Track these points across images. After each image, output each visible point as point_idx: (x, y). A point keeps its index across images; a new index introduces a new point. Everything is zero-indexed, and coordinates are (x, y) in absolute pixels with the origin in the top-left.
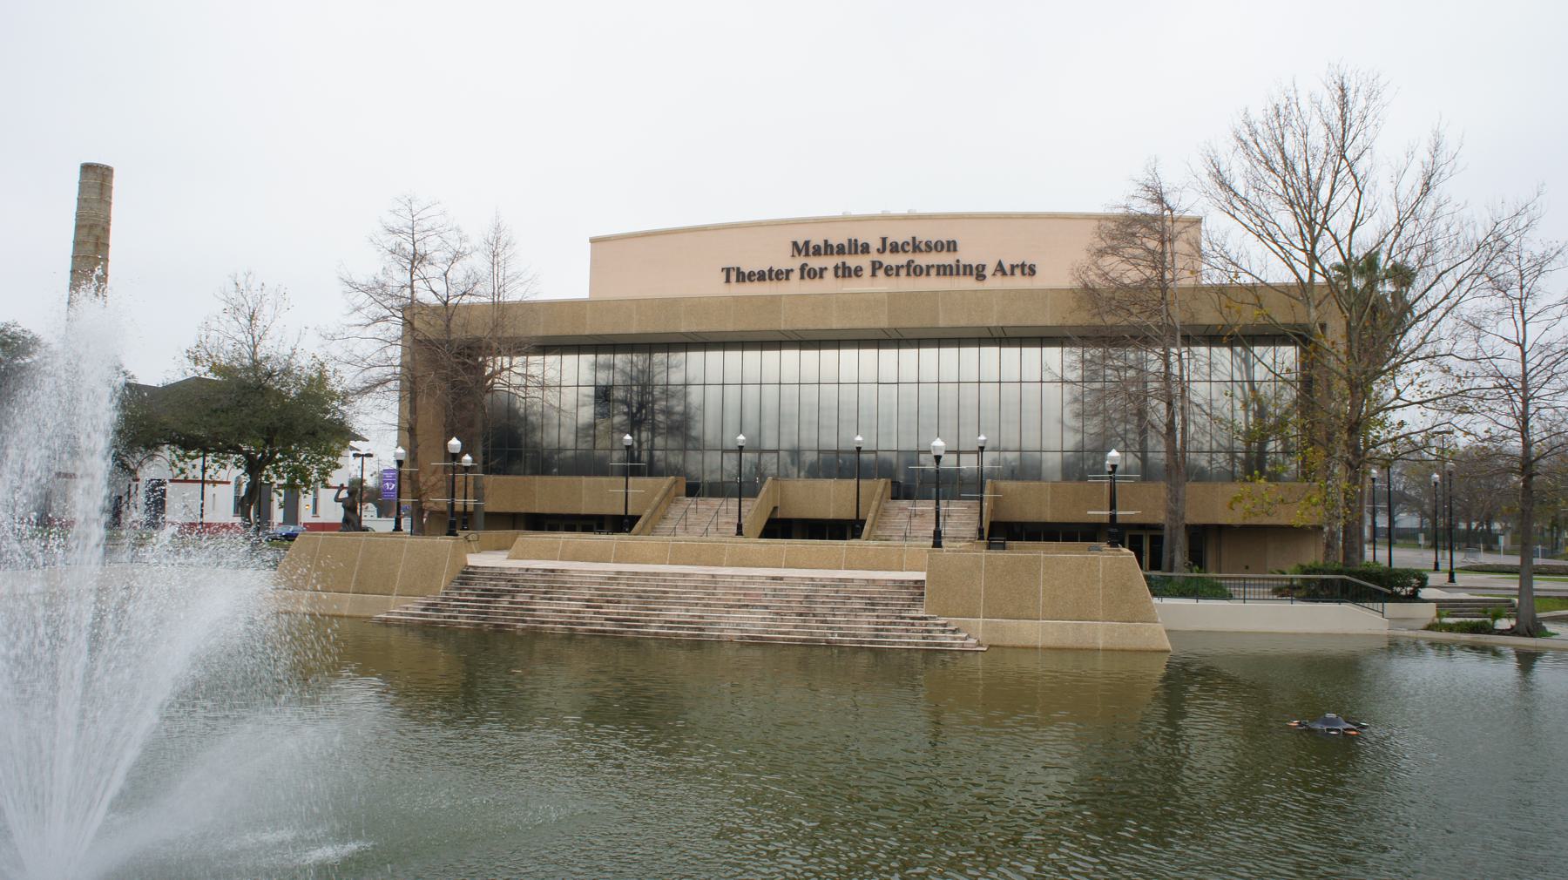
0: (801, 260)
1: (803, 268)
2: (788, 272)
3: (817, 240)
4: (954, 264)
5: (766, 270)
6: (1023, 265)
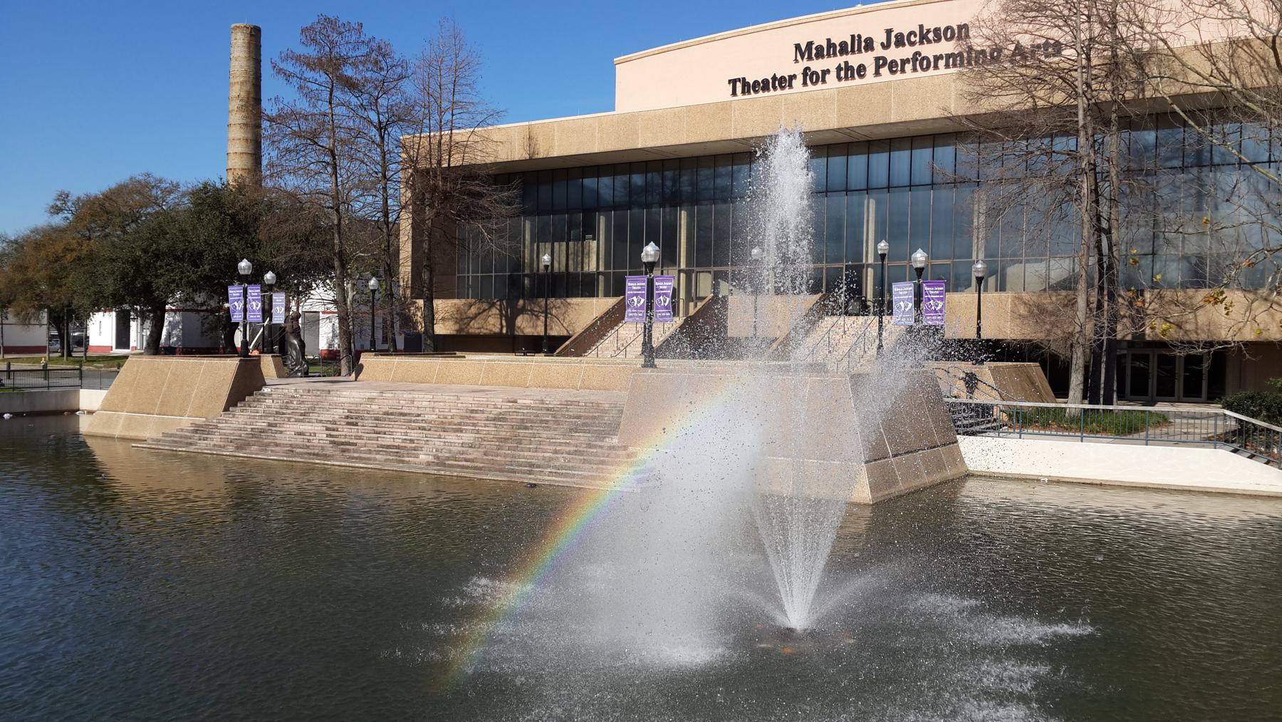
0: (805, 63)
2: (793, 77)
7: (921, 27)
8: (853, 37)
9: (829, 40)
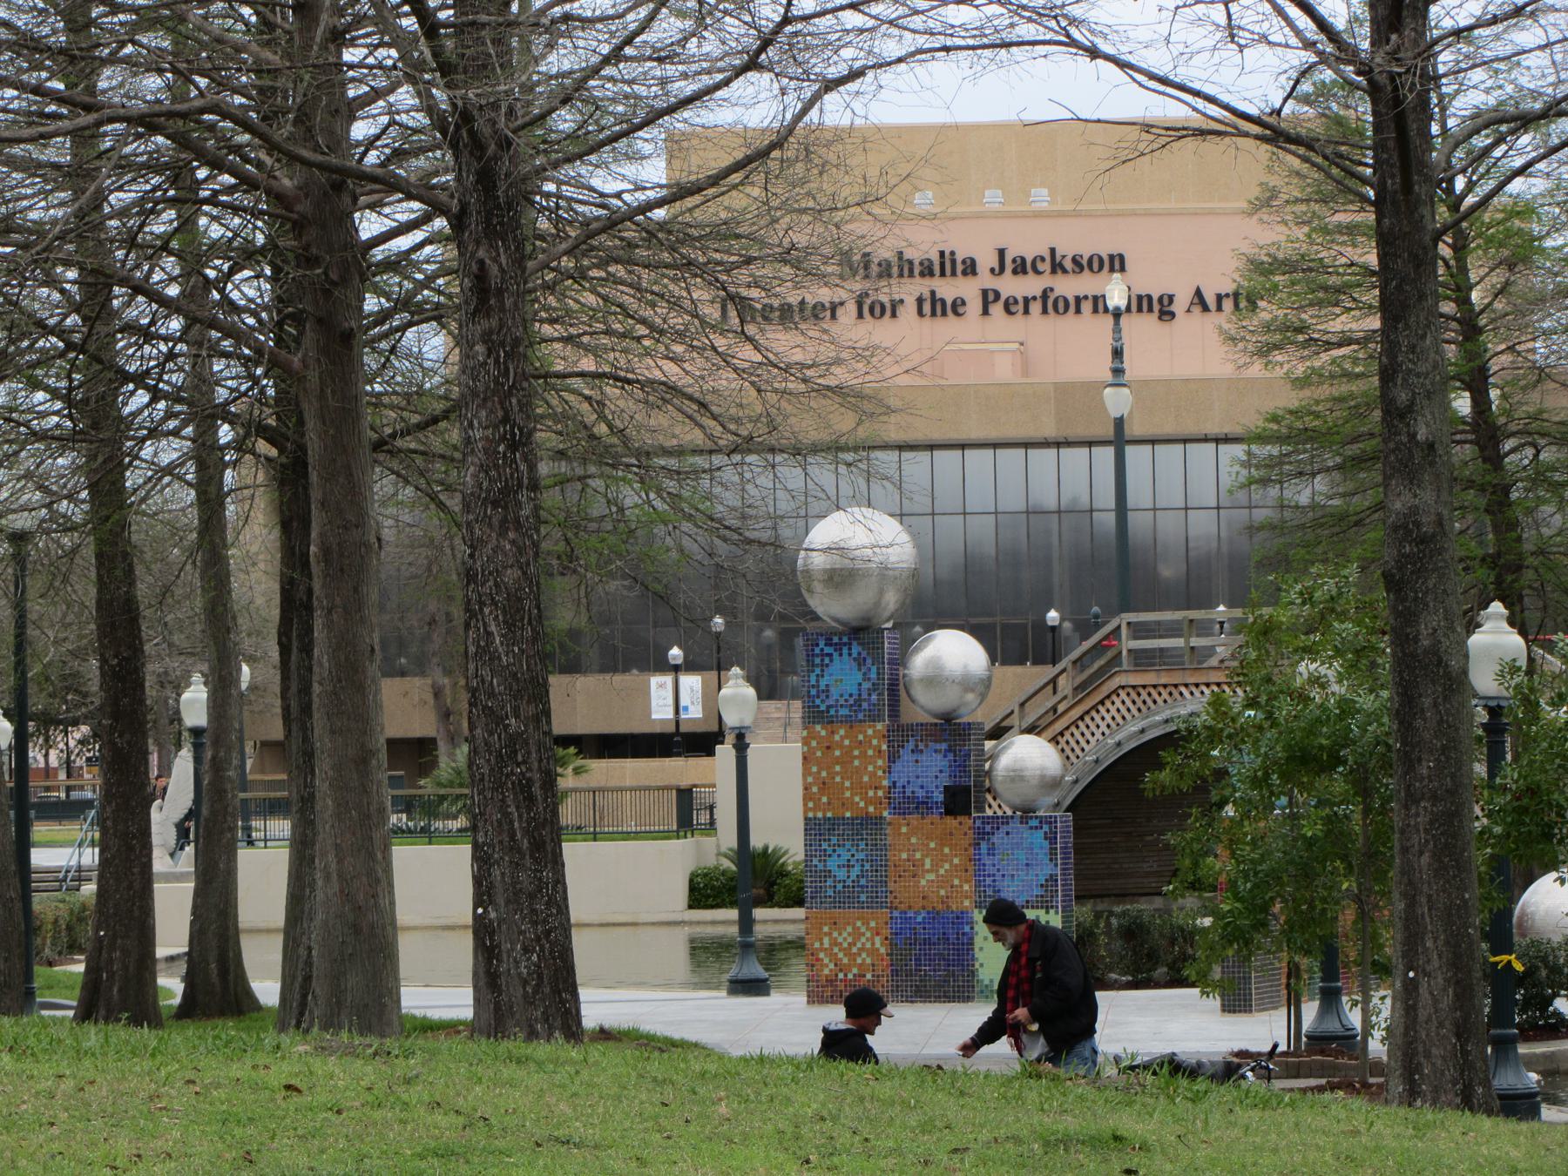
7: (1053, 251)
8: (942, 254)
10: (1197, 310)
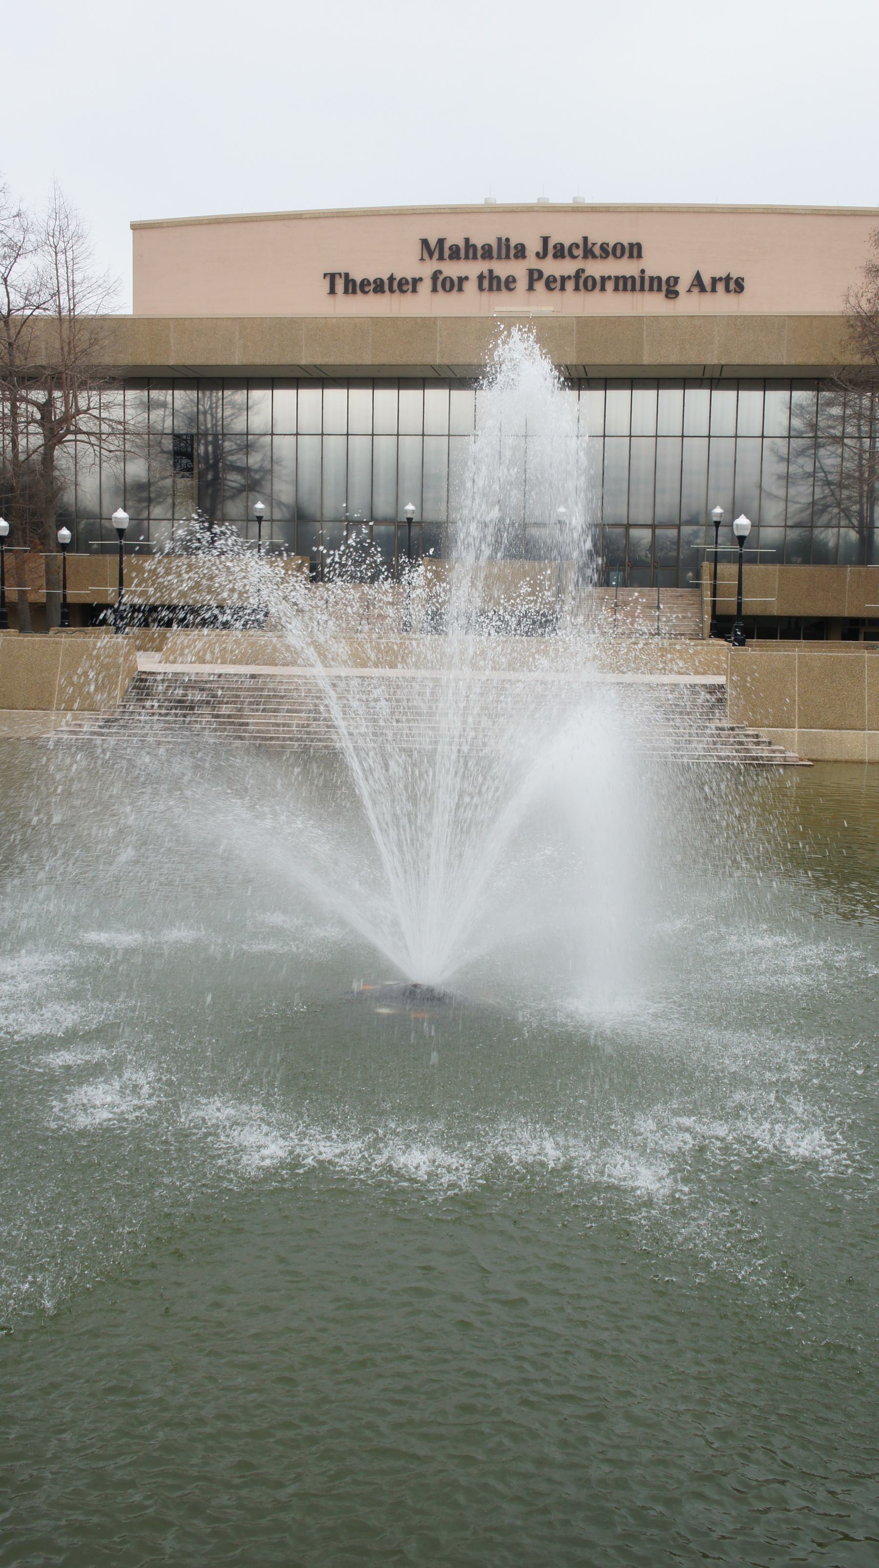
0: (433, 265)
1: (435, 276)
2: (416, 281)
3: (455, 238)
4: (637, 275)
5: (385, 278)
6: (728, 279)
7: (585, 239)
8: (499, 240)
9: (467, 240)
10: (696, 290)
